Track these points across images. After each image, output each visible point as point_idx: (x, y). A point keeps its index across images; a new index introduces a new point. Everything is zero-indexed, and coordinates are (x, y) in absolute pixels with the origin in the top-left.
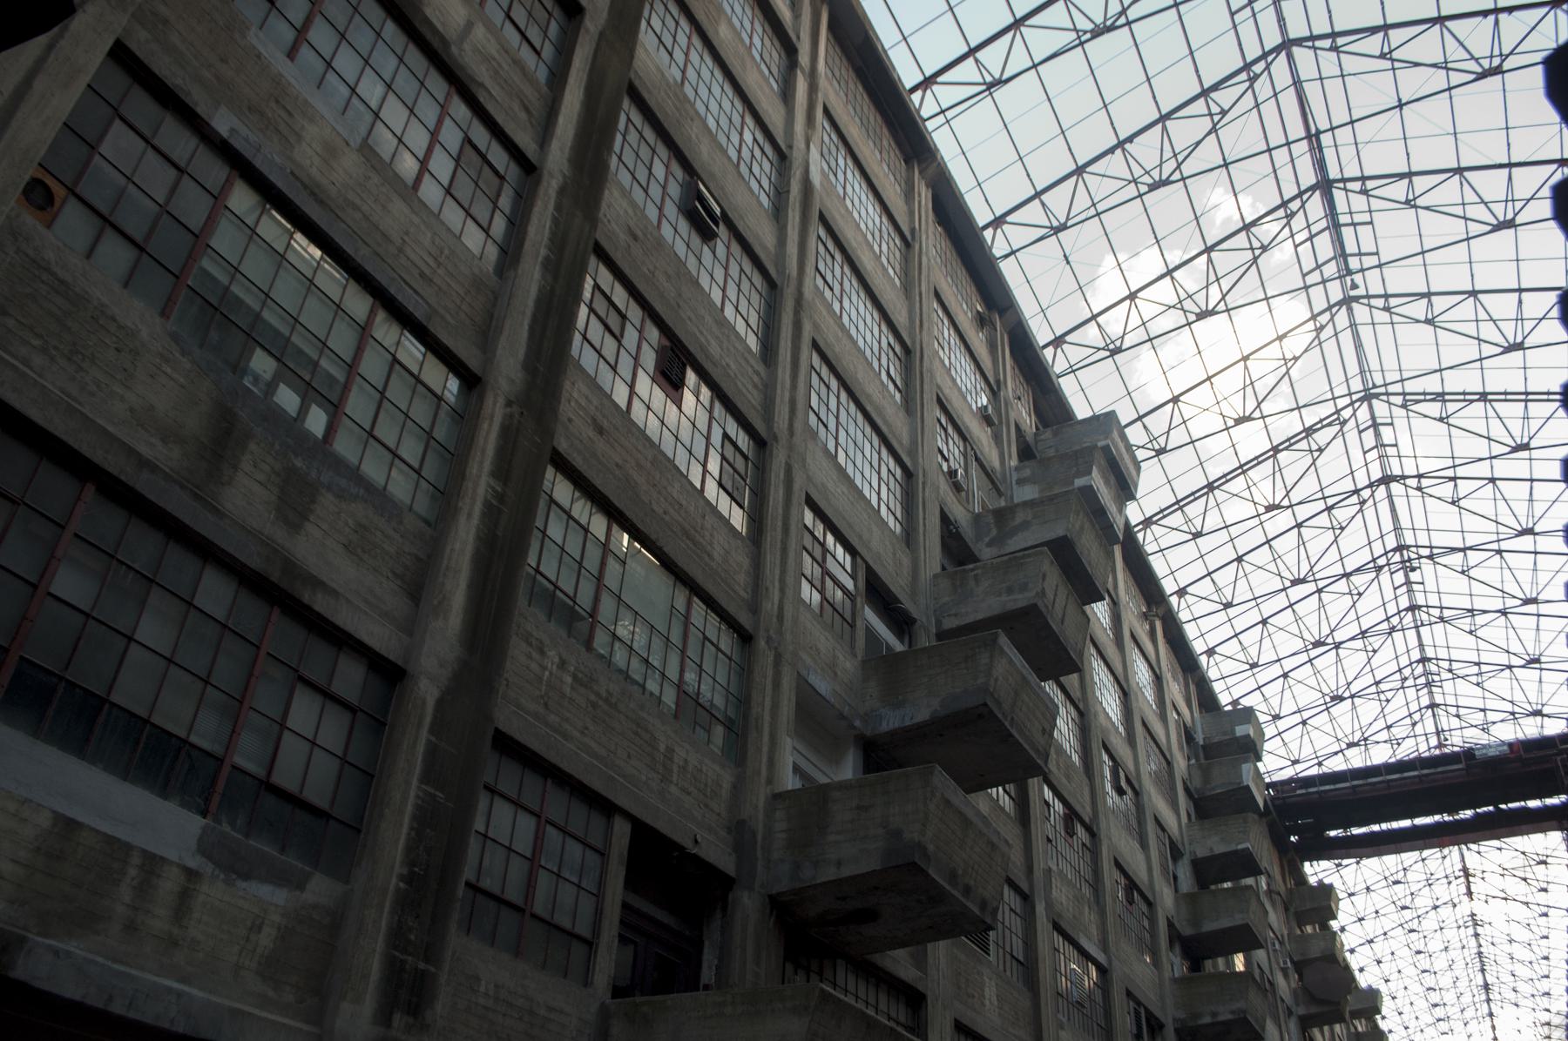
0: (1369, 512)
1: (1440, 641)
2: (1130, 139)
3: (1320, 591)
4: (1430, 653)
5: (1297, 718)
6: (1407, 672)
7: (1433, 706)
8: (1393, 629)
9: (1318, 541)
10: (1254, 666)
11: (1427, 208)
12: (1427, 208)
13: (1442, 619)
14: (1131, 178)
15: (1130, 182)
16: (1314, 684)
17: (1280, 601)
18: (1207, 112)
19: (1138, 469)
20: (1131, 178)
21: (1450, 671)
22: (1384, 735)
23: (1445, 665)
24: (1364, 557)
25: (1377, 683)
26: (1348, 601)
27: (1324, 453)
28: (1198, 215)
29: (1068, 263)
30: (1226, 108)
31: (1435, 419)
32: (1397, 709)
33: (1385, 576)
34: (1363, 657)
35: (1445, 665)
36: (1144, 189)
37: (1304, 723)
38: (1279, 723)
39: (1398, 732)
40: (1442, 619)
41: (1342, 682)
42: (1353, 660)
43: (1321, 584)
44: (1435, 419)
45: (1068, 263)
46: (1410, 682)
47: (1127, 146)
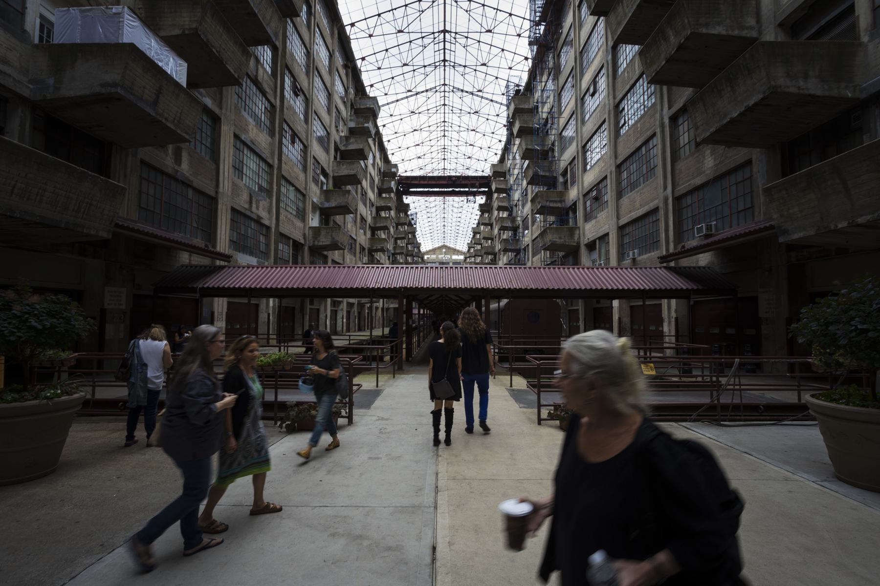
0: (437, 70)
1: (450, 117)
3: (414, 70)
5: (400, 117)
6: (439, 125)
7: (444, 105)
8: (436, 91)
9: (420, 78)
10: (391, 115)
13: (453, 91)
16: (403, 85)
17: (399, 71)
19: (380, 109)
21: (452, 110)
22: (427, 129)
23: (450, 125)
24: (433, 86)
25: (428, 110)
26: (423, 76)
32: (434, 135)
33: (438, 93)
34: (425, 99)
35: (450, 125)
37: (401, 119)
38: (393, 117)
39: (433, 143)
40: (453, 91)
41: (419, 124)
43: (415, 68)
46: (439, 129)
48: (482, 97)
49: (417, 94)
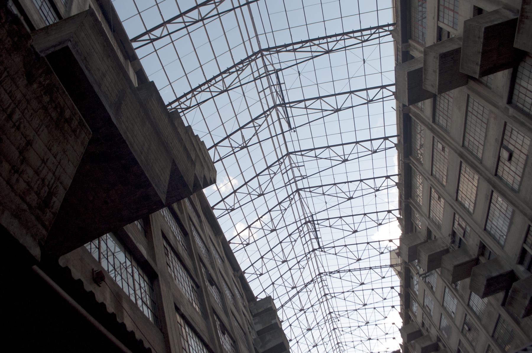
2: (261, 217)
4: (331, 310)
11: (328, 195)
12: (328, 195)
14: (248, 193)
15: (248, 194)
18: (268, 174)
20: (248, 193)
27: (305, 269)
28: (278, 234)
29: (246, 251)
30: (286, 208)
31: (333, 254)
36: (289, 289)
42: (310, 315)
44: (333, 254)
45: (246, 251)
47: (261, 219)
48: (360, 269)
49: (298, 292)
